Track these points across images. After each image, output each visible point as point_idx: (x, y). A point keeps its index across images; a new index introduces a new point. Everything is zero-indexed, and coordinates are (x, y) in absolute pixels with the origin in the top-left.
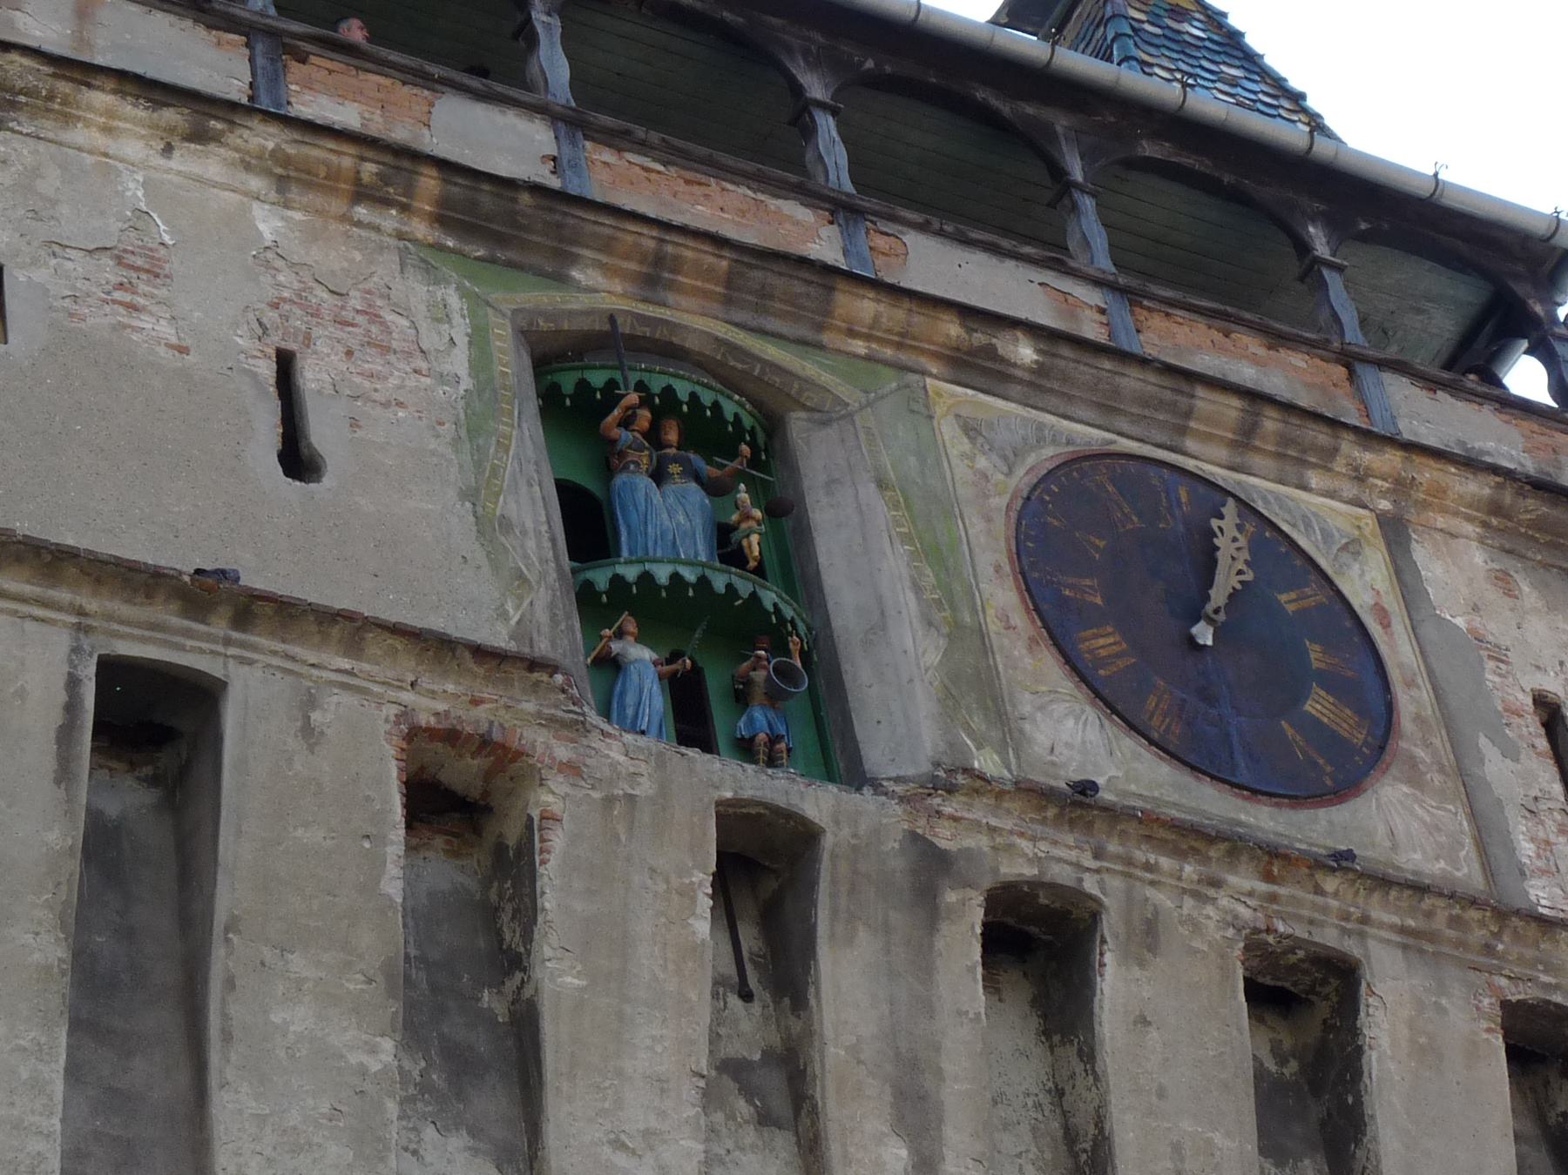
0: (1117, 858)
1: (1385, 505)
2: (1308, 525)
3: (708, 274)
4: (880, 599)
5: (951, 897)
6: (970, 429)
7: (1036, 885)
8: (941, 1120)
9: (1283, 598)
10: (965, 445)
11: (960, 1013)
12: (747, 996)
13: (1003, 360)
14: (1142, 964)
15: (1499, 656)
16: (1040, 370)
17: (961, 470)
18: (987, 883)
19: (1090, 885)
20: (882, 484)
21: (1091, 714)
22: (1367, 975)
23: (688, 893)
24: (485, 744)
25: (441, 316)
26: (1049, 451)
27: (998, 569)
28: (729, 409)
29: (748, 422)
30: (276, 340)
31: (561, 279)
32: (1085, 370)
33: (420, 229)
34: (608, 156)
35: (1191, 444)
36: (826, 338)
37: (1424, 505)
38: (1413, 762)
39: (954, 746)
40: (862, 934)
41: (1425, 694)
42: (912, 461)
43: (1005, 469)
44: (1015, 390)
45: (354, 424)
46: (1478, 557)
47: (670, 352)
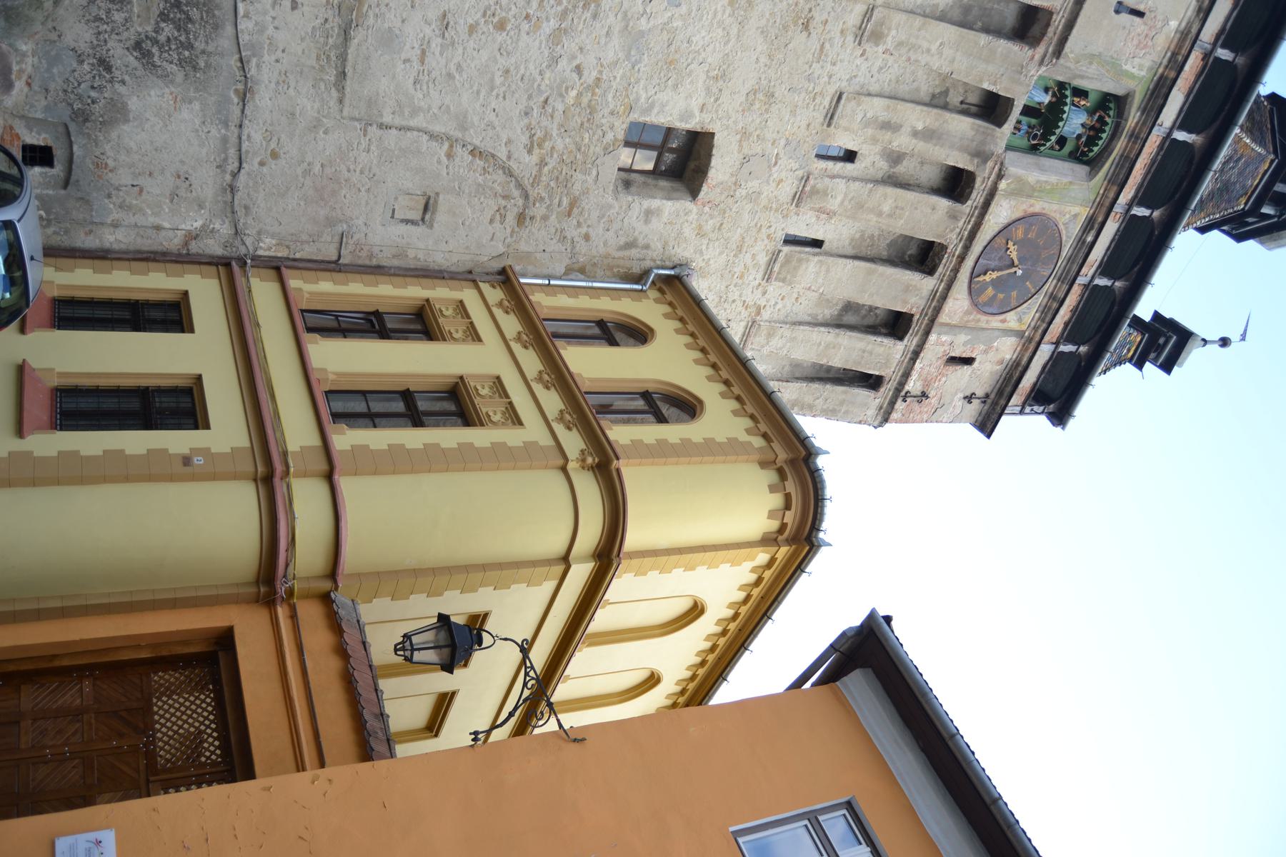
0: (974, 212)
1: (1027, 334)
2: (1029, 309)
3: (1130, 151)
4: (1046, 171)
5: (976, 161)
6: (1076, 216)
7: (973, 188)
8: (925, 142)
9: (1015, 293)
10: (1073, 213)
11: (948, 156)
12: (962, 102)
13: (1089, 232)
14: (947, 213)
15: (986, 352)
16: (1084, 242)
17: (1068, 209)
18: (977, 173)
19: (969, 203)
20: (1071, 183)
22: (930, 277)
23: (995, 84)
24: (1043, 34)
26: (1064, 238)
27: (1044, 209)
28: (1096, 149)
29: (1091, 154)
30: (1147, 14)
32: (1081, 255)
33: (1161, 70)
34: (1158, 143)
35: (1055, 281)
36: (1106, 182)
37: (1023, 346)
40: (973, 133)
41: (984, 325)
42: (1073, 195)
44: (1080, 234)
45: (1124, 28)
46: (1008, 357)
47: (1114, 136)
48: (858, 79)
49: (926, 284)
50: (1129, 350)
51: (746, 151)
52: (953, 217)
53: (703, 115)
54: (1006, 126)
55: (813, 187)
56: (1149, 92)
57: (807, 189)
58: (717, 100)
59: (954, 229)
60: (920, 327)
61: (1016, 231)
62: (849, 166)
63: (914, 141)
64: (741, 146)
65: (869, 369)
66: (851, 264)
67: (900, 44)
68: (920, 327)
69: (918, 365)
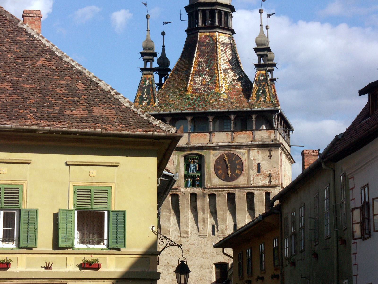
2: (241, 153)
6: (213, 155)
17: (212, 159)
19: (215, 193)
21: (218, 178)
25: (176, 158)
27: (213, 168)
31: (185, 152)
34: (192, 134)
35: (232, 149)
38: (244, 174)
39: (207, 185)
40: (200, 199)
41: (247, 167)
43: (215, 157)
44: (218, 150)
48: (196, 233)
49: (237, 193)
50: (262, 75)
51: (216, 255)
52: (219, 195)
53: (210, 268)
54: (196, 193)
55: (221, 234)
56: (180, 151)
57: (222, 235)
58: (206, 266)
59: (222, 194)
60: (249, 190)
61: (219, 173)
62: (215, 226)
63: (205, 213)
64: (215, 256)
65: (263, 198)
66: (237, 215)
67: (187, 226)
68: (249, 190)
69: (260, 184)
